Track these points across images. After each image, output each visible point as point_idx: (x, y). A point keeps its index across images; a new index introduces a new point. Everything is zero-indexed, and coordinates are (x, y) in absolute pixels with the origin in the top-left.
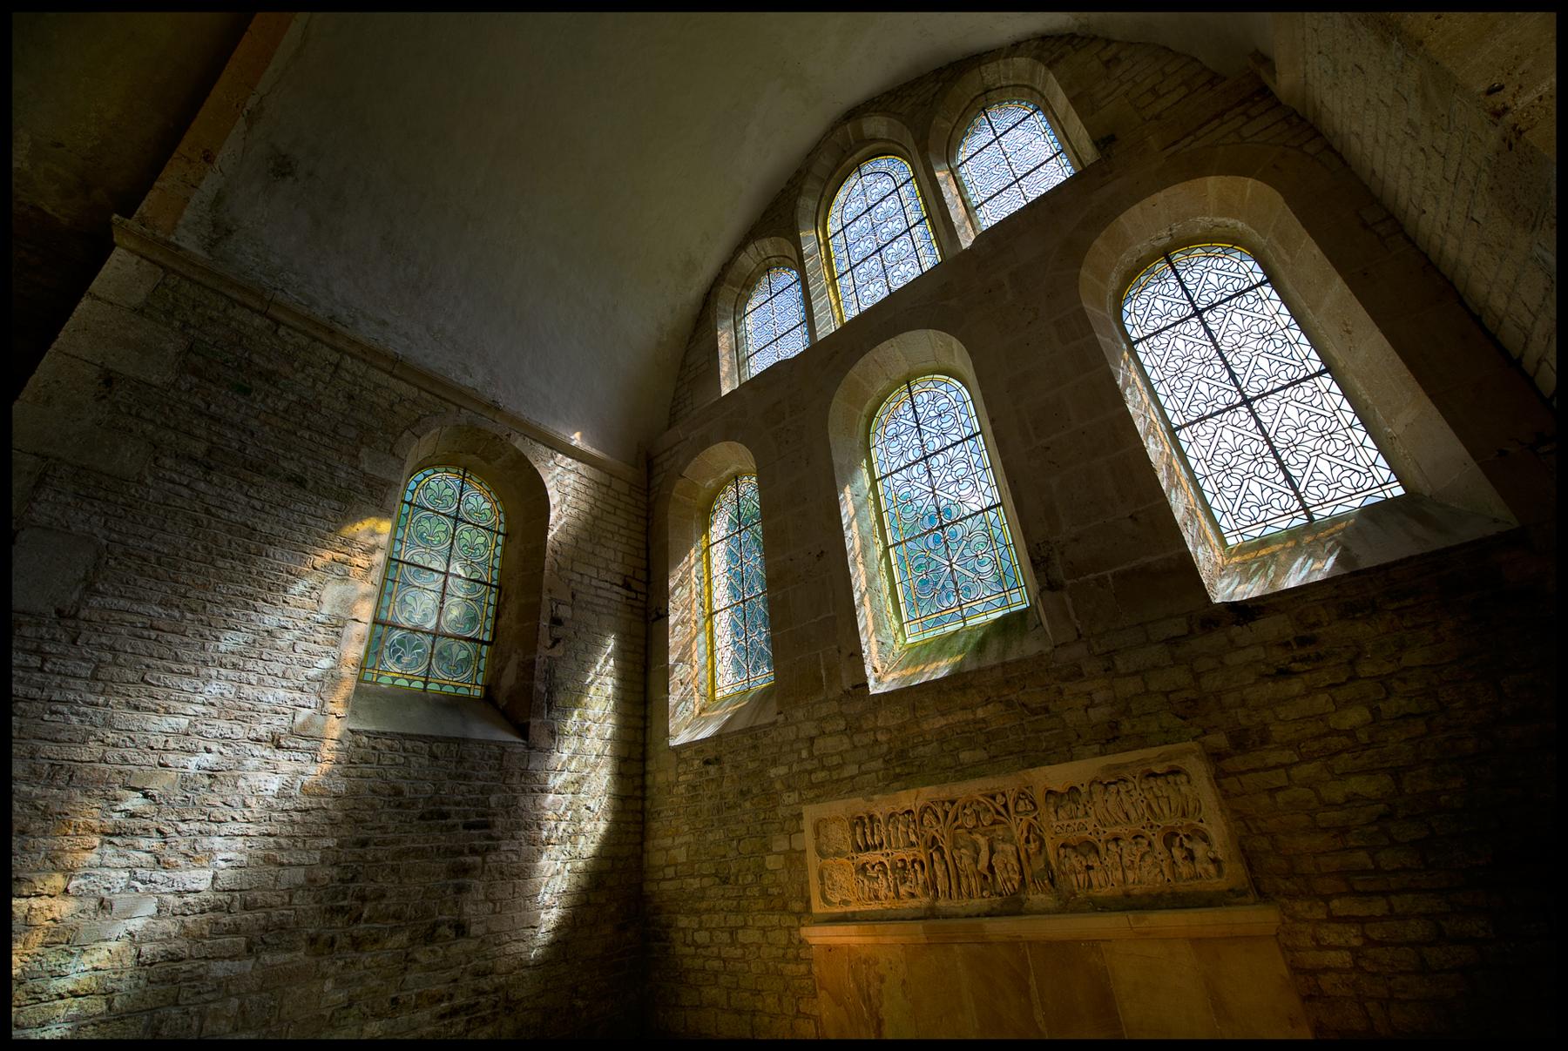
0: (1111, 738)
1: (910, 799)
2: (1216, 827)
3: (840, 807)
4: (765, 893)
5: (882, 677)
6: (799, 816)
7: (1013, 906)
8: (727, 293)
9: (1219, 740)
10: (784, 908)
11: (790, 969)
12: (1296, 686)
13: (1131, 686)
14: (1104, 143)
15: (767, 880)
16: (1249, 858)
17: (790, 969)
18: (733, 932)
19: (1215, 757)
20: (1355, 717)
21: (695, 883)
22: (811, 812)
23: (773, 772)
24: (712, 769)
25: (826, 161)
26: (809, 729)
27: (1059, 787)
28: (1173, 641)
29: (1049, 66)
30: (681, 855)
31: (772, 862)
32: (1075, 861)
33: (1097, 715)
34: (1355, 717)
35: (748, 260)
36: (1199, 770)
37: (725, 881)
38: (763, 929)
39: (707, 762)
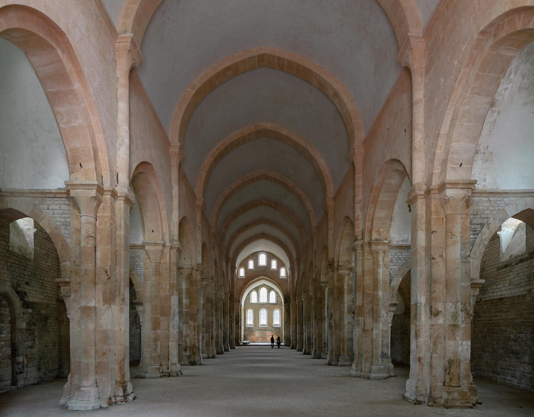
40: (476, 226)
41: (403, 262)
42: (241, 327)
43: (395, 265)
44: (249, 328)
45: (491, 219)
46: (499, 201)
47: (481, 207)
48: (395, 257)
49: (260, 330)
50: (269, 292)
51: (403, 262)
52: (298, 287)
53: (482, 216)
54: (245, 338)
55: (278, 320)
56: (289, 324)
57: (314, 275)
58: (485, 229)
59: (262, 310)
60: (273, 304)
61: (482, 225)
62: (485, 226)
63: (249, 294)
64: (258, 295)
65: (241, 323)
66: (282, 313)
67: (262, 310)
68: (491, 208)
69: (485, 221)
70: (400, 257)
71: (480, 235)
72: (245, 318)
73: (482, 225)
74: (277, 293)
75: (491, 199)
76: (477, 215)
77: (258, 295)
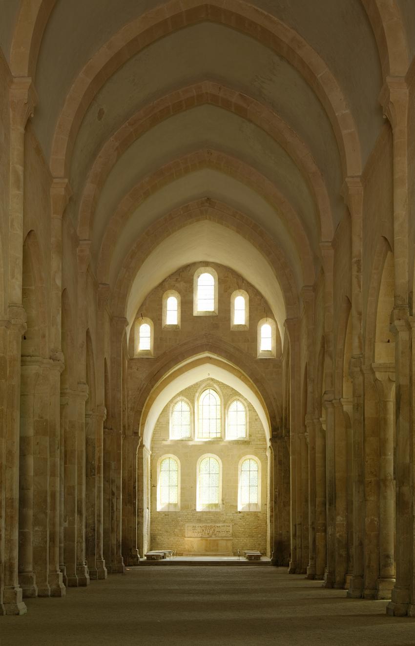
0: (224, 522)
1: (201, 525)
2: (231, 531)
3: (192, 525)
4: (174, 534)
5: (199, 508)
6: (184, 525)
7: (211, 537)
8: (172, 405)
9: (233, 524)
10: (178, 536)
11: (178, 543)
12: (241, 520)
13: (227, 517)
14: (250, 436)
15: (175, 532)
16: (232, 534)
17: (178, 543)
18: (168, 538)
19: (233, 525)
20: (244, 524)
21: (161, 532)
22: (187, 525)
23: (179, 519)
24: (167, 517)
25: (204, 385)
26: (186, 514)
27: (218, 526)
28: (233, 514)
29: (249, 410)
30: (160, 528)
31: (176, 530)
32: (218, 533)
33: (224, 519)
34: (244, 524)
35: (178, 399)
36: (231, 526)
37: (167, 532)
38: (174, 538)
39: (166, 515)
42: (141, 510)
44: (166, 514)
49: (199, 521)
50: (226, 405)
52: (310, 389)
54: (153, 544)
55: (252, 490)
56: (287, 504)
57: (356, 342)
59: (207, 458)
60: (238, 443)
63: (165, 411)
64: (193, 413)
65: (141, 500)
66: (264, 469)
67: (207, 458)
72: (154, 486)
74: (250, 408)
77: (193, 413)
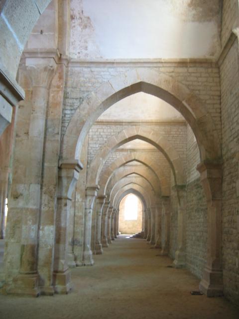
40: (75, 101)
41: (105, 139)
43: (95, 144)
45: (93, 93)
46: (104, 72)
47: (82, 79)
48: (97, 133)
51: (105, 139)
53: (82, 89)
58: (84, 104)
61: (81, 99)
62: (85, 101)
68: (93, 80)
69: (85, 95)
70: (102, 134)
71: (78, 110)
73: (81, 99)
75: (93, 69)
76: (76, 88)
